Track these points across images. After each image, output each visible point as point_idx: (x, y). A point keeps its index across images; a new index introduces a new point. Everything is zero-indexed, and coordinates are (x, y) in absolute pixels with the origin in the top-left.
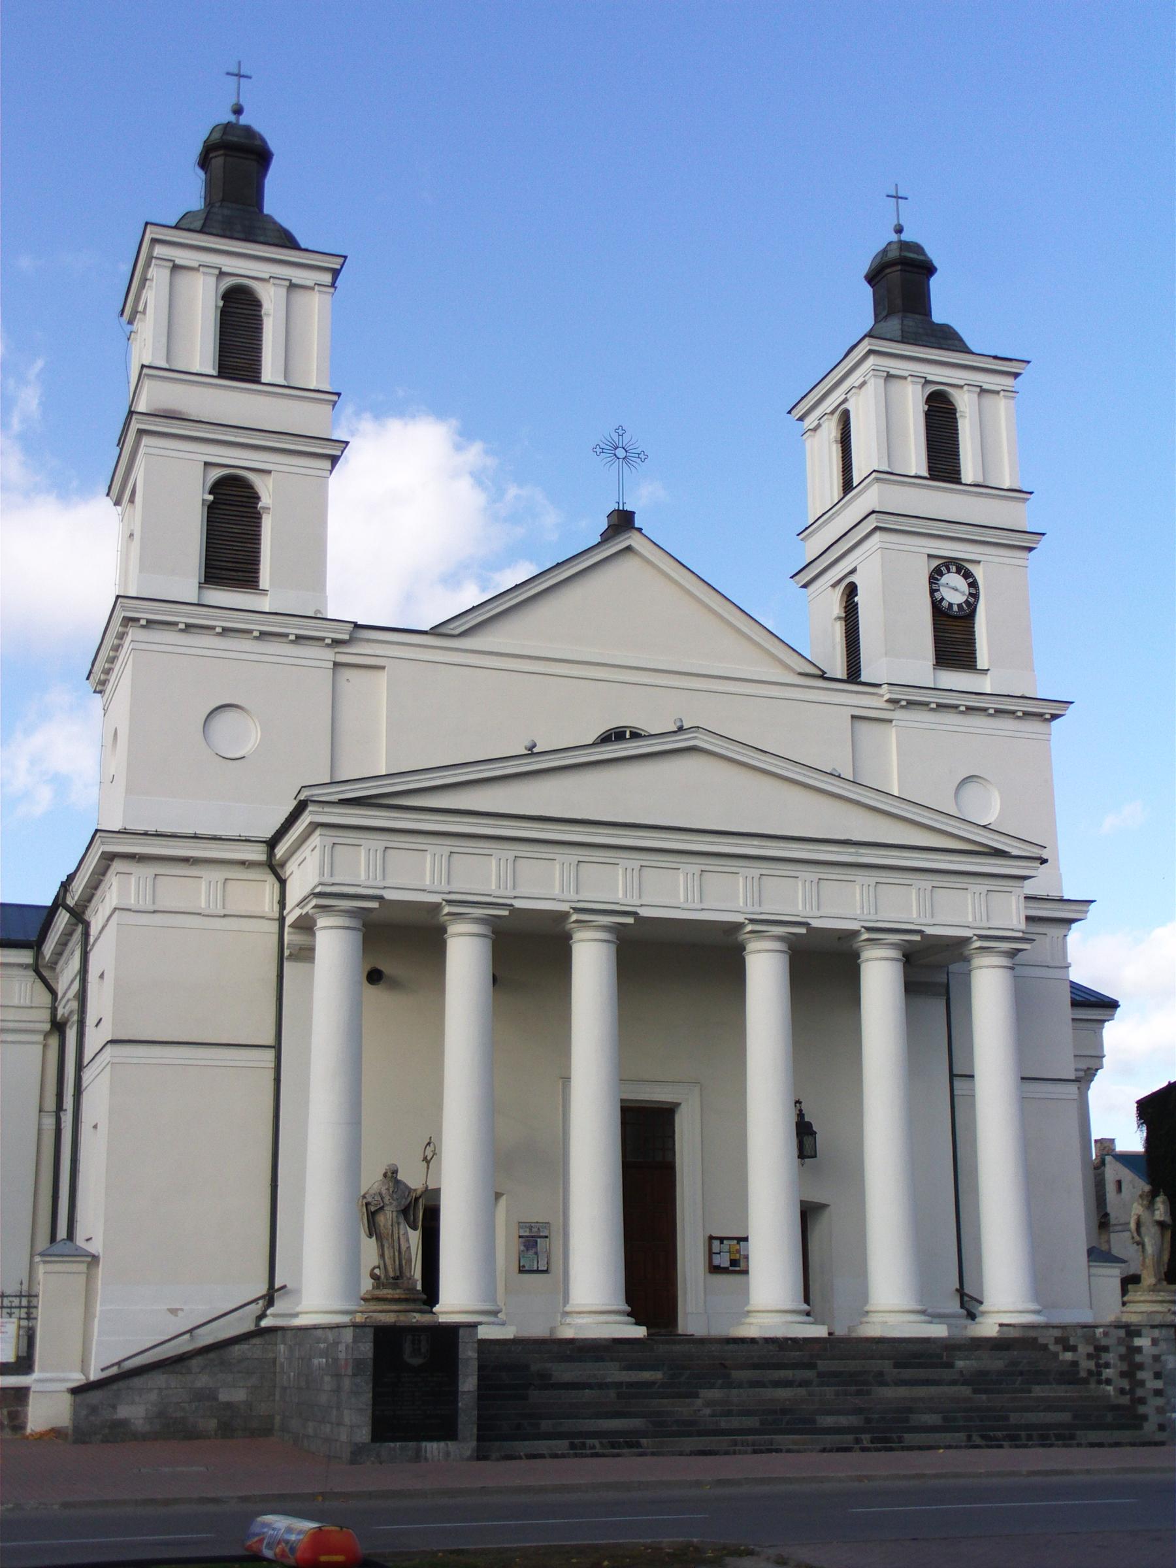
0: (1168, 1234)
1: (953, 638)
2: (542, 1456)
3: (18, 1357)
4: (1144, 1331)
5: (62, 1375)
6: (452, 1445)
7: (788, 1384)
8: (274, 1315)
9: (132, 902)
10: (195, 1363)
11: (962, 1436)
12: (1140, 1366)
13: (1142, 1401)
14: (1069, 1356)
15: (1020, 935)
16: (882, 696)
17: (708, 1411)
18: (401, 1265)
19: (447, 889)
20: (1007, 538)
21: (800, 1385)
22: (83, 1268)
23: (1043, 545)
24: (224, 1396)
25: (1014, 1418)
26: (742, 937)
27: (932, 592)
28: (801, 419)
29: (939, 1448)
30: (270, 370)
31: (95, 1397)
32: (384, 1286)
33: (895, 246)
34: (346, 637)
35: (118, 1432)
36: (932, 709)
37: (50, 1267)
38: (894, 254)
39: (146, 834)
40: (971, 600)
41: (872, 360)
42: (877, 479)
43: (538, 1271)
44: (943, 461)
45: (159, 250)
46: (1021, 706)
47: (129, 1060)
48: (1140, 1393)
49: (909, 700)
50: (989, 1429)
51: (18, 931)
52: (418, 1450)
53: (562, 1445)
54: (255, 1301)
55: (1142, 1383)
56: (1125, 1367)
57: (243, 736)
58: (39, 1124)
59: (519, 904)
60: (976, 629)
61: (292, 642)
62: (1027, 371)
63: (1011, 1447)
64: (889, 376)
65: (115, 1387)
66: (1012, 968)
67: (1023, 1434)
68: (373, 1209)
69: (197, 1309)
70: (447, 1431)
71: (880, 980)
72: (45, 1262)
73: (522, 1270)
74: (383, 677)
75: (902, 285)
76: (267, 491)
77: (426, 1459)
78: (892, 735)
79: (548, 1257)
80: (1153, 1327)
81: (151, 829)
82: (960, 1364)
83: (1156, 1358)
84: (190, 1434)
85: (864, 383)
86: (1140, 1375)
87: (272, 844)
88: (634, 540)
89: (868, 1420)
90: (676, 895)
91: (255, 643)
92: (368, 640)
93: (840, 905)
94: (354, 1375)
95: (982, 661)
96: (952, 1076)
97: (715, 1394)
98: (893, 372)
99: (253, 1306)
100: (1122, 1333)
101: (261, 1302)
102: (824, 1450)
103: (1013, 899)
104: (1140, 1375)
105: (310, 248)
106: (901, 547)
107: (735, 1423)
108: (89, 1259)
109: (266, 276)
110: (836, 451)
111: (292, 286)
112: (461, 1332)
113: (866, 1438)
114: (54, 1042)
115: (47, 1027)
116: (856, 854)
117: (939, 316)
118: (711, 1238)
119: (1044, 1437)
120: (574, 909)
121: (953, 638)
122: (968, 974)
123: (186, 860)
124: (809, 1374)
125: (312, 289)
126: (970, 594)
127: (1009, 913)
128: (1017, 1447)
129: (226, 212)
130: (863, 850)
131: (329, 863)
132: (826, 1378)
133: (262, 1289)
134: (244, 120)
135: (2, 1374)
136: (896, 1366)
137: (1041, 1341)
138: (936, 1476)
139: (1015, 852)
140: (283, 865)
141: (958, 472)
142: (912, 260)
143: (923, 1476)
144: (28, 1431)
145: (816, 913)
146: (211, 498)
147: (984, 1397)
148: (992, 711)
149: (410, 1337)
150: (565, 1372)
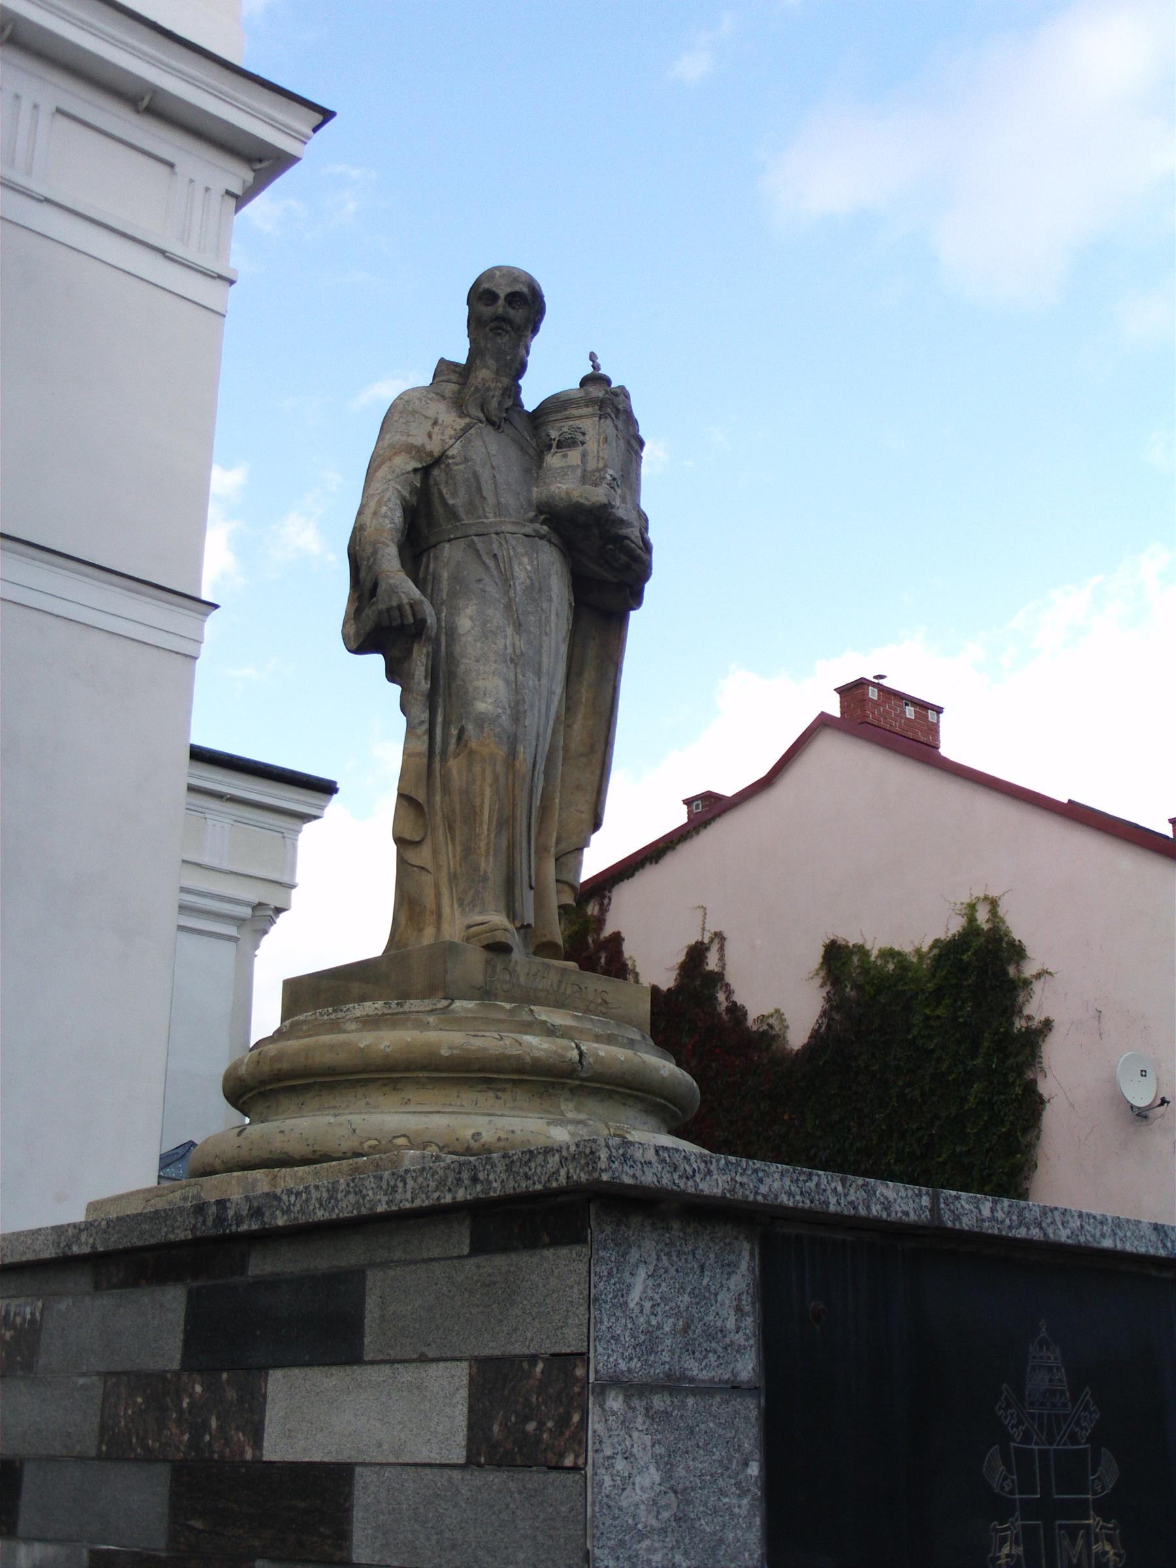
100: (154, 1326)
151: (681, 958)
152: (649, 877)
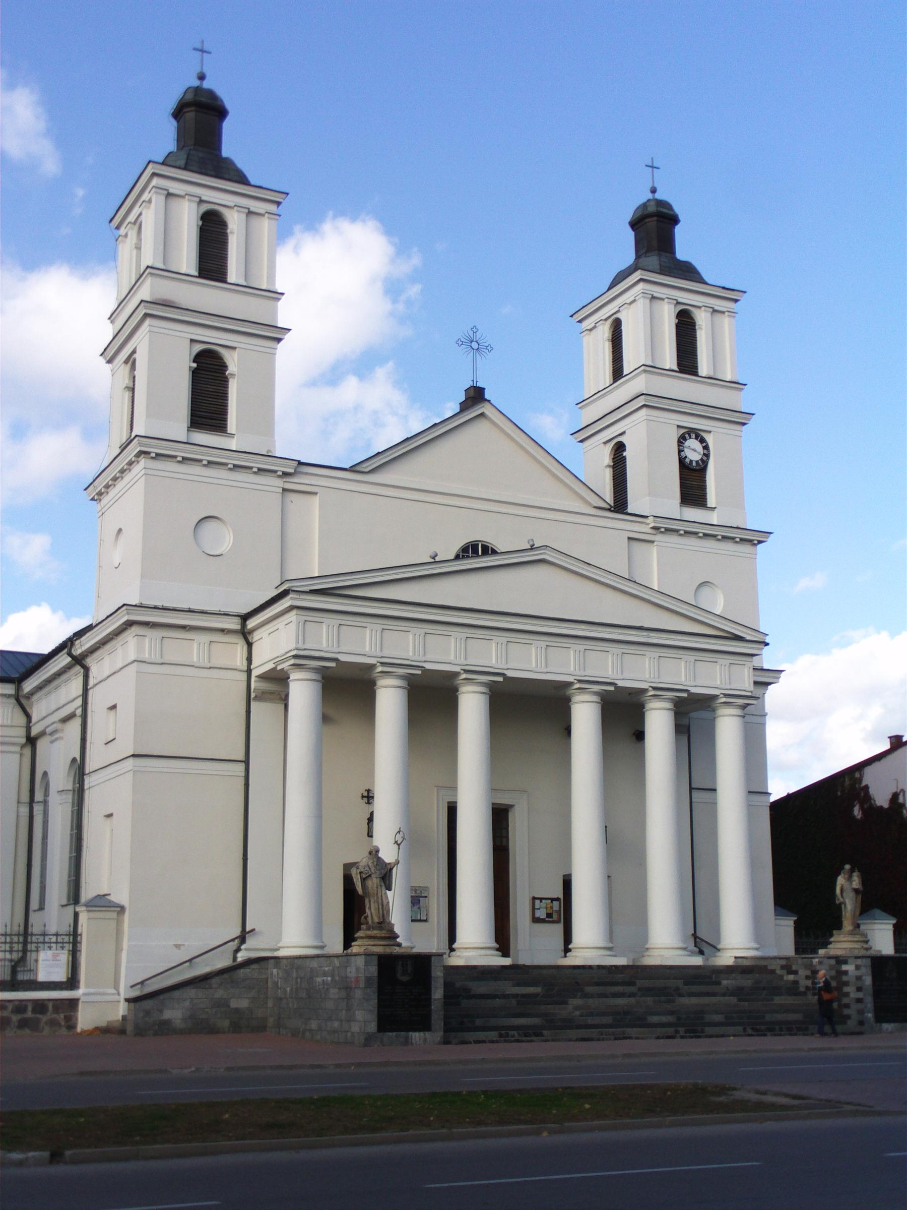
0: (860, 897)
1: (692, 484)
2: (484, 1042)
3: (68, 978)
4: (849, 961)
5: (101, 990)
6: (428, 1034)
7: (622, 995)
8: (246, 949)
9: (146, 656)
10: (215, 981)
11: (740, 1028)
12: (846, 984)
13: (847, 1006)
14: (791, 977)
15: (749, 694)
16: (648, 524)
17: (578, 1013)
18: (383, 916)
19: (380, 654)
20: (729, 416)
21: (629, 996)
22: (114, 915)
23: (753, 422)
24: (234, 1004)
25: (768, 1017)
26: (644, 698)
27: (680, 451)
28: (580, 321)
29: (729, 1036)
30: (234, 273)
31: (148, 1004)
32: (374, 929)
33: (652, 203)
34: (292, 471)
35: (164, 1028)
36: (681, 535)
37: (92, 915)
38: (652, 208)
39: (156, 608)
40: (705, 458)
41: (641, 286)
42: (645, 371)
43: (420, 921)
44: (687, 361)
45: (155, 181)
46: (738, 535)
47: (146, 769)
48: (845, 1001)
49: (666, 528)
50: (758, 1025)
51: (14, 671)
52: (407, 1038)
53: (493, 1035)
54: (233, 940)
55: (847, 995)
57: (222, 539)
58: (18, 812)
59: (428, 666)
60: (707, 479)
61: (255, 473)
62: (744, 299)
63: (772, 1035)
64: (653, 298)
65: (162, 997)
66: (744, 717)
67: (777, 1027)
68: (364, 876)
69: (195, 946)
70: (425, 1026)
71: (658, 723)
72: (89, 911)
73: (413, 921)
74: (316, 499)
75: (655, 229)
76: (233, 363)
77: (412, 1044)
78: (654, 550)
79: (427, 911)
80: (857, 957)
81: (159, 604)
82: (725, 982)
83: (859, 978)
84: (213, 1030)
85: (634, 301)
86: (846, 989)
87: (245, 618)
88: (486, 409)
89: (679, 1019)
90: (530, 662)
91: (204, 469)
92: (306, 474)
93: (635, 671)
94: (366, 988)
95: (711, 501)
96: (691, 789)
97: (578, 1002)
98: (655, 295)
99: (231, 943)
100: (833, 962)
101: (236, 941)
102: (658, 1038)
103: (746, 670)
104: (846, 989)
105: (264, 186)
106: (661, 420)
107: (597, 1020)
108: (119, 909)
109: (232, 204)
110: (607, 347)
111: (250, 213)
112: (433, 959)
113: (682, 1030)
114: (28, 751)
115: (24, 740)
116: (648, 637)
117: (682, 253)
118: (534, 898)
119: (789, 1029)
120: (464, 670)
121: (692, 484)
122: (714, 720)
123: (183, 627)
124: (628, 989)
125: (263, 215)
126: (704, 454)
127: (744, 681)
128: (775, 1035)
129: (201, 155)
130: (652, 634)
131: (302, 634)
132: (648, 991)
133: (237, 932)
134: (206, 85)
135: (2, 990)
136: (686, 983)
137: (769, 968)
138: (755, 1051)
139: (749, 638)
140: (252, 631)
141: (696, 368)
142: (665, 214)
143: (747, 1051)
144: (79, 1030)
145: (620, 677)
146: (195, 365)
147: (746, 1003)
148: (682, 532)
149: (400, 962)
150: (480, 988)
151: (890, 797)
152: (876, 765)
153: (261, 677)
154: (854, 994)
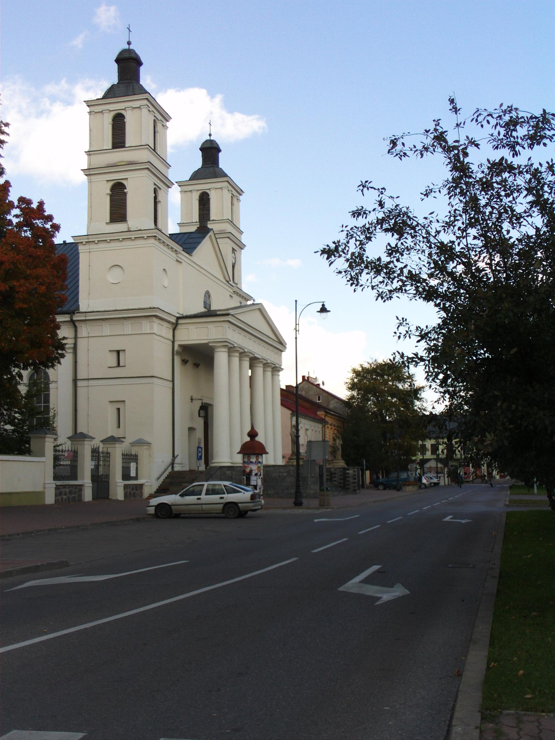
12: (348, 477)
13: (348, 485)
48: (347, 483)
55: (349, 481)
56: (342, 477)
86: (347, 479)
87: (178, 318)
104: (347, 479)
153: (180, 346)
154: (351, 480)
